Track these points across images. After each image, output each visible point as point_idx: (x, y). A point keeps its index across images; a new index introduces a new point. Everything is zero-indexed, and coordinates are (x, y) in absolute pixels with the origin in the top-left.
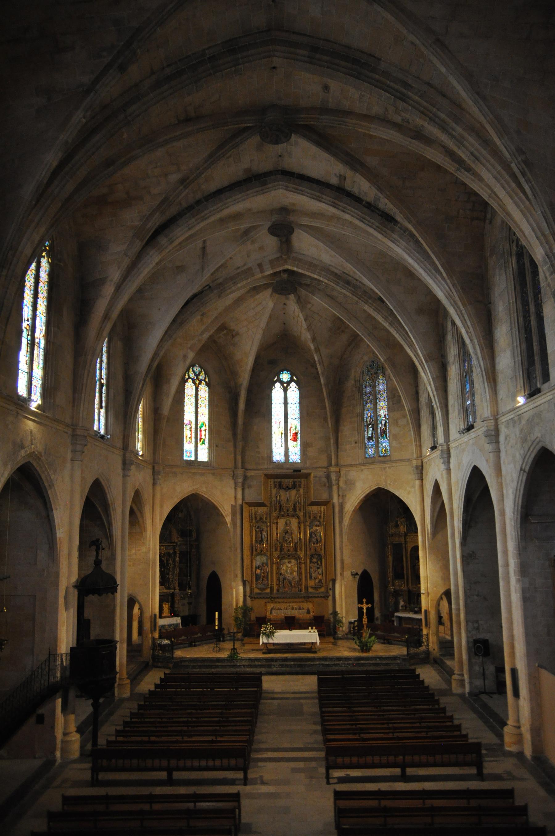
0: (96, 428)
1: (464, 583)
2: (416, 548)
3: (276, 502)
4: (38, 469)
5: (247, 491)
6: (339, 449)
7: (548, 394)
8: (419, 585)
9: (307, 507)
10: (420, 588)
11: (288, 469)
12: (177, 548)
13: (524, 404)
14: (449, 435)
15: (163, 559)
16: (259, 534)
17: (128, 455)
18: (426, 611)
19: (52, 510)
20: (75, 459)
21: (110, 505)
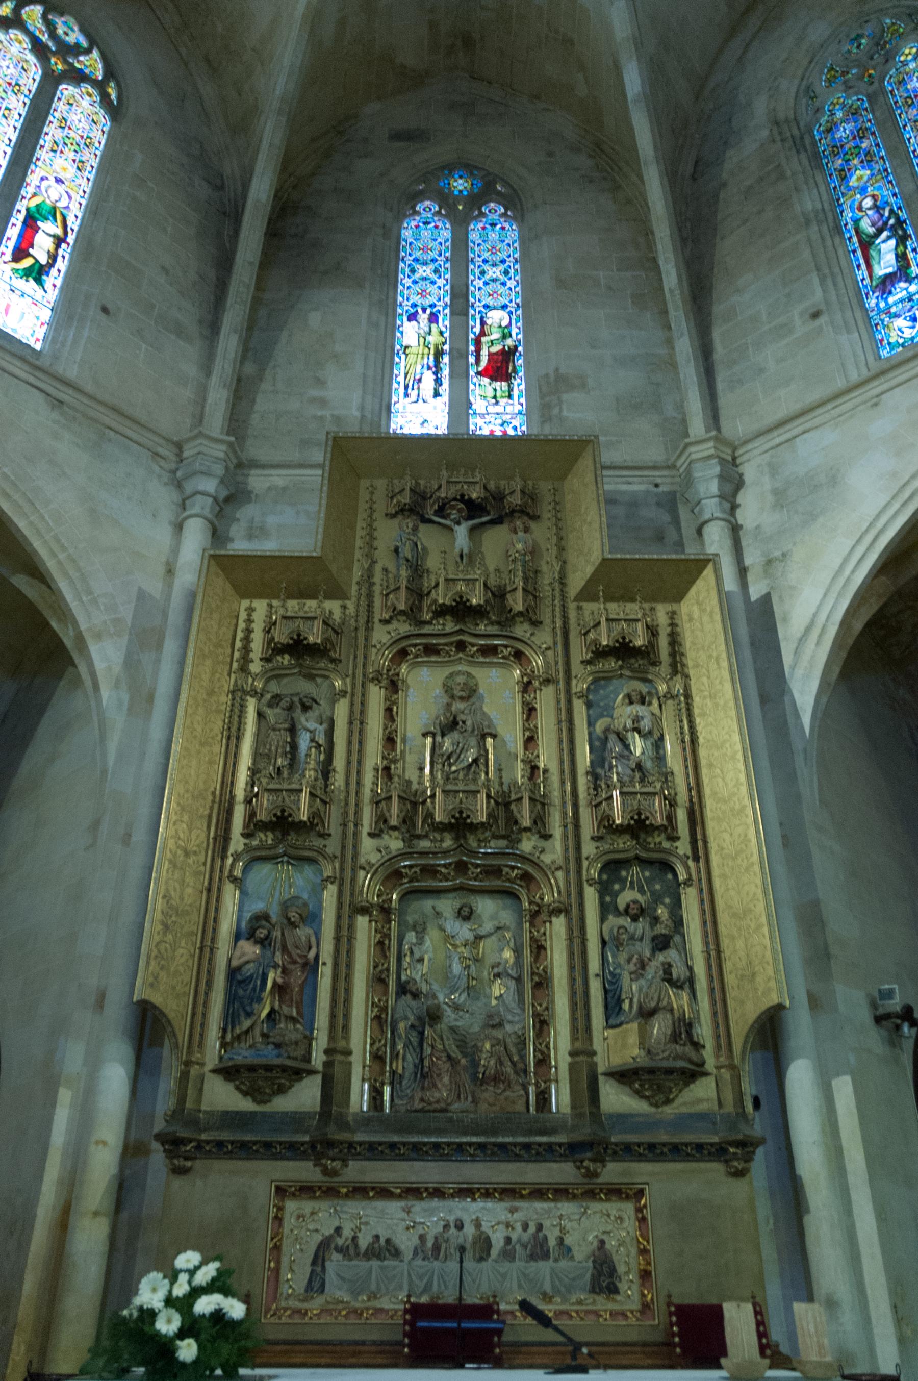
16: (278, 739)
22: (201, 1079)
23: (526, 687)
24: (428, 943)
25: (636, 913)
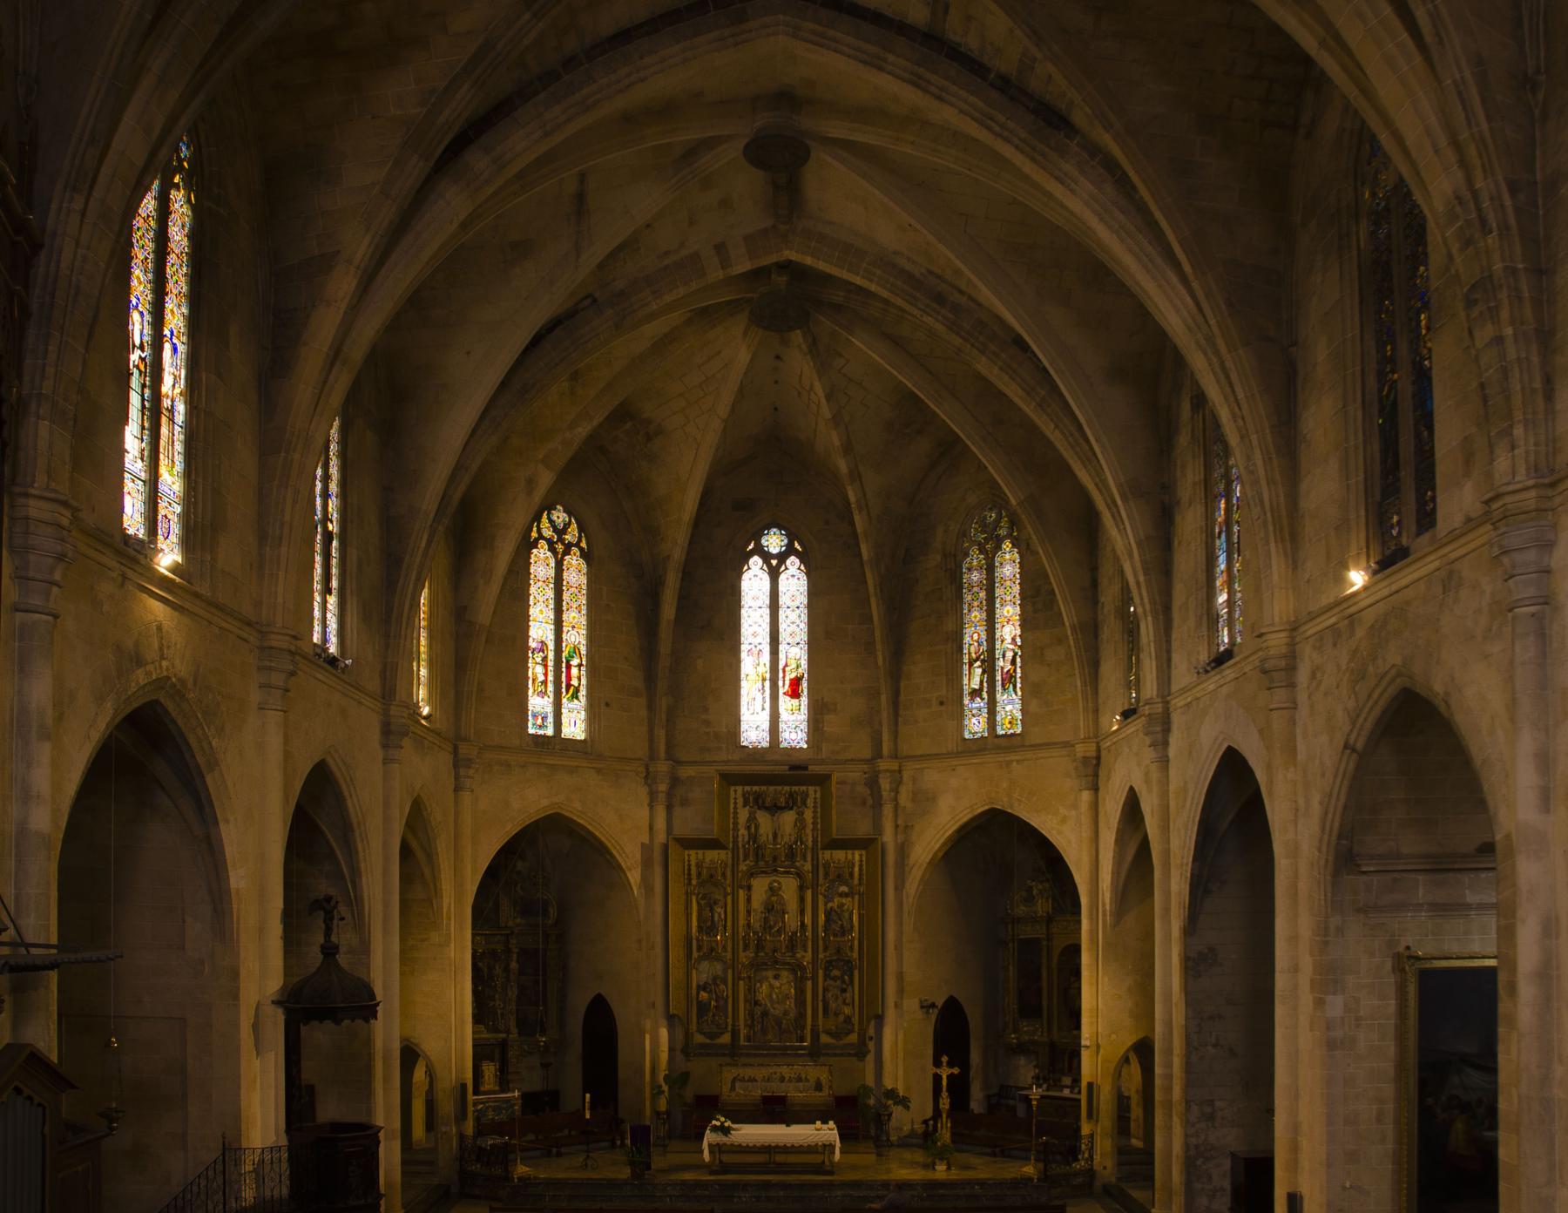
0: (316, 638)
1: (1187, 1018)
2: (1077, 949)
3: (746, 839)
4: (180, 722)
6: (900, 719)
7: (1432, 557)
8: (1075, 1032)
9: (820, 853)
10: (1079, 1037)
11: (776, 763)
12: (513, 941)
13: (1365, 588)
14: (1169, 678)
15: (480, 964)
16: (707, 913)
17: (394, 711)
18: (1090, 1085)
19: (216, 823)
20: (266, 707)
21: (355, 825)
22: (692, 1034)
24: (764, 987)
25: (834, 979)
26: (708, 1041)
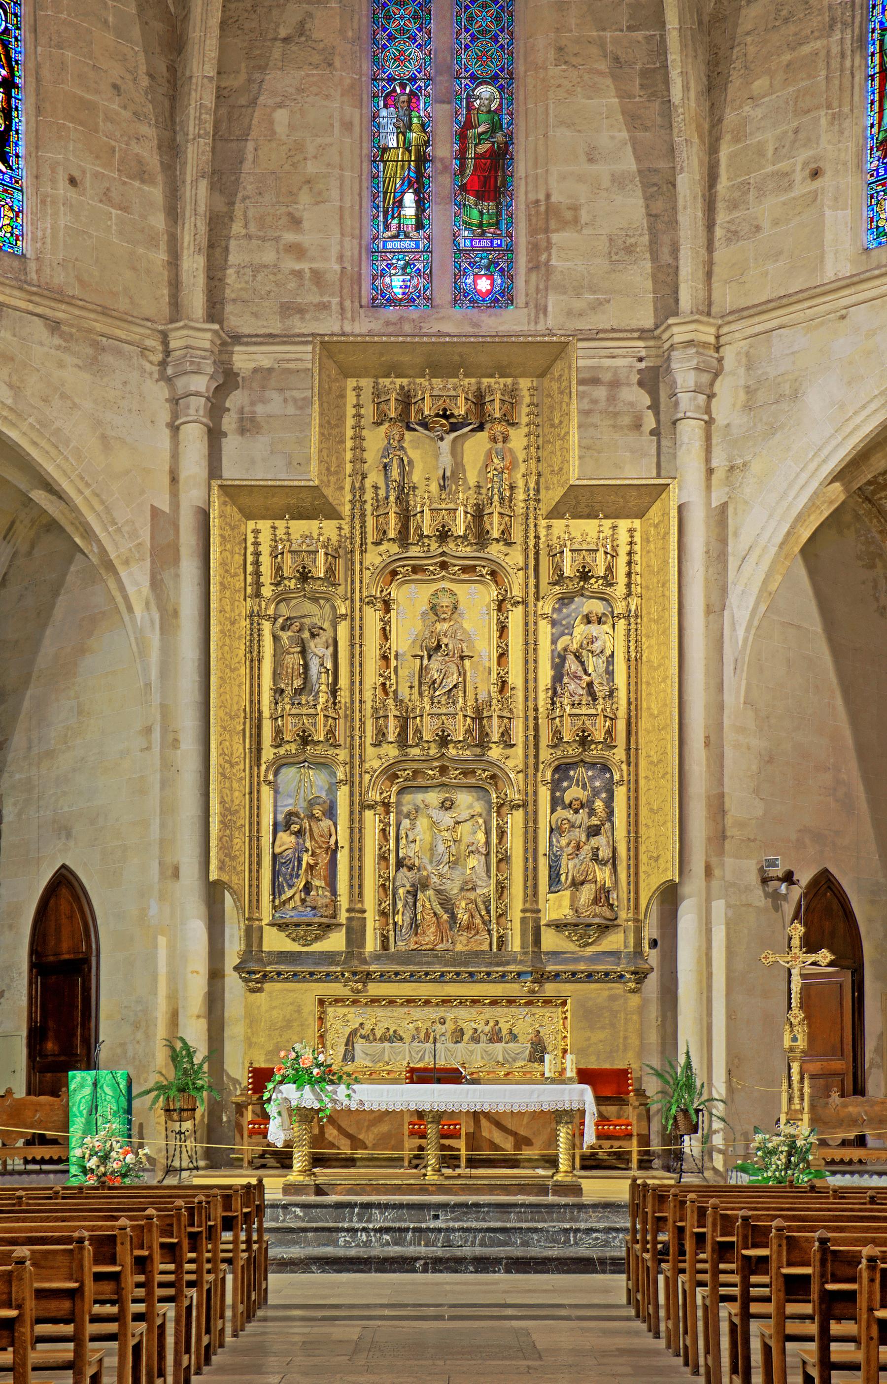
5: (231, 445)
16: (293, 660)
22: (261, 929)
23: (500, 605)
25: (576, 807)
26: (295, 947)
